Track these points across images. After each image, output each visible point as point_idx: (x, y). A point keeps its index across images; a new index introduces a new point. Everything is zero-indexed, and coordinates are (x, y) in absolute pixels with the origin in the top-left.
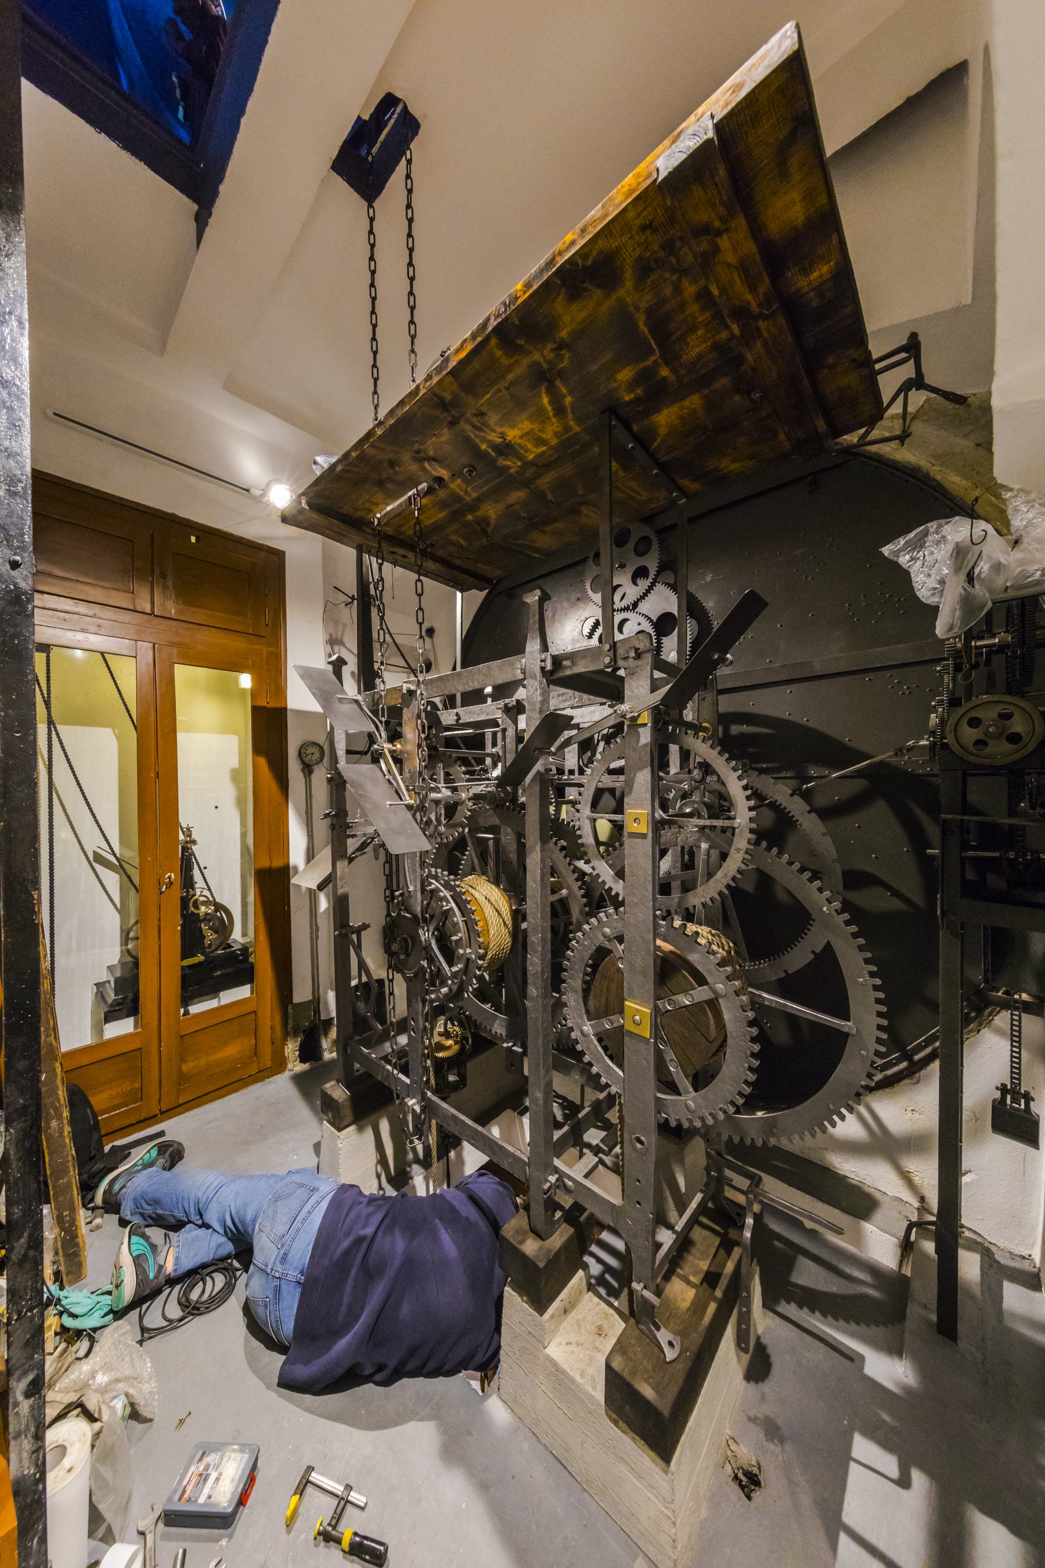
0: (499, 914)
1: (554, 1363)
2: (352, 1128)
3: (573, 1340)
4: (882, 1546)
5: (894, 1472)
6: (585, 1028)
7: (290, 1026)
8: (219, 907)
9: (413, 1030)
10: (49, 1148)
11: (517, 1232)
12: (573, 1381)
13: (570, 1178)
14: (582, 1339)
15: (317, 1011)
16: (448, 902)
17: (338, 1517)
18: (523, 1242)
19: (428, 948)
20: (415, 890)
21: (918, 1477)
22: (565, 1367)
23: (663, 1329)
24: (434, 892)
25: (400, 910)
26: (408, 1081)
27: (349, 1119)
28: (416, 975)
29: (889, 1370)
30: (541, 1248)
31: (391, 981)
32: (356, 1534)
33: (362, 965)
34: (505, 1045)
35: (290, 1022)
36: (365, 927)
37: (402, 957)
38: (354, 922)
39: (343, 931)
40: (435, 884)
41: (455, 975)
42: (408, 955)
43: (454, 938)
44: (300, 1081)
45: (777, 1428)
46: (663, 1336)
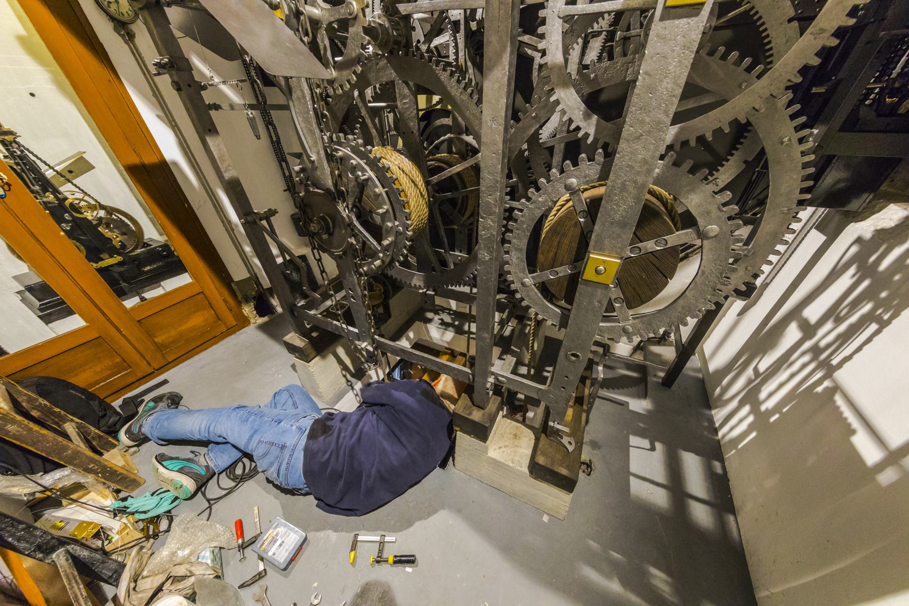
0: (415, 185)
1: (494, 460)
2: (317, 359)
3: (502, 445)
4: (648, 476)
5: (648, 446)
6: (526, 280)
7: (240, 297)
8: (110, 210)
9: (352, 297)
10: (27, 444)
11: (465, 408)
12: (508, 466)
13: (503, 376)
14: (507, 443)
15: (258, 283)
16: (364, 171)
17: (381, 551)
18: (470, 414)
19: (351, 224)
20: (320, 158)
21: (658, 445)
22: (502, 460)
23: (564, 437)
24: (343, 160)
25: (307, 185)
26: (356, 330)
27: (314, 354)
28: (345, 253)
29: (639, 406)
30: (484, 415)
31: (319, 260)
32: (396, 556)
33: (283, 249)
34: (421, 291)
35: (238, 294)
36: (272, 213)
37: (325, 237)
38: (259, 208)
39: (250, 219)
40: (342, 151)
41: (385, 249)
42: (331, 234)
43: (381, 211)
44: (262, 328)
45: (596, 443)
46: (565, 440)
